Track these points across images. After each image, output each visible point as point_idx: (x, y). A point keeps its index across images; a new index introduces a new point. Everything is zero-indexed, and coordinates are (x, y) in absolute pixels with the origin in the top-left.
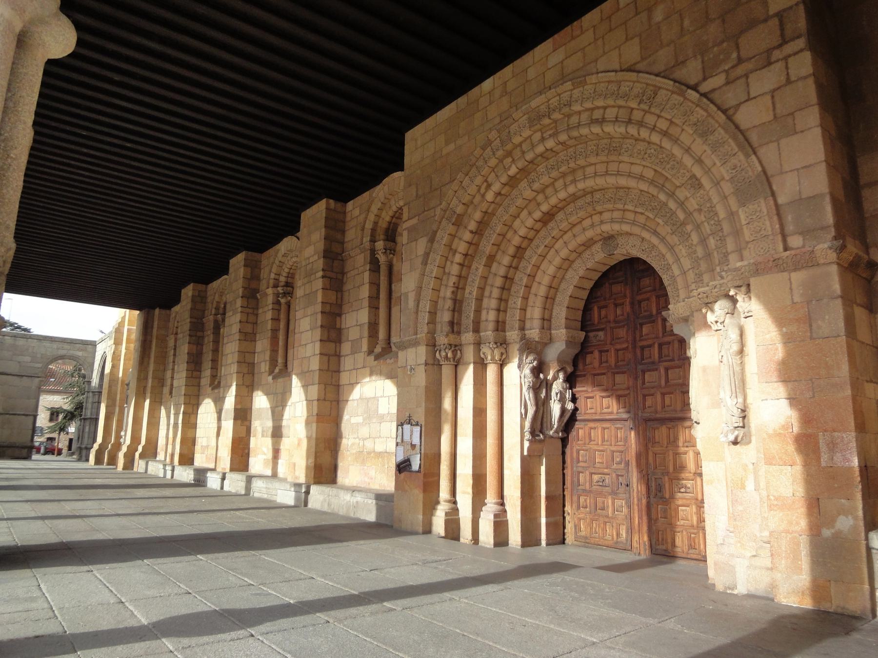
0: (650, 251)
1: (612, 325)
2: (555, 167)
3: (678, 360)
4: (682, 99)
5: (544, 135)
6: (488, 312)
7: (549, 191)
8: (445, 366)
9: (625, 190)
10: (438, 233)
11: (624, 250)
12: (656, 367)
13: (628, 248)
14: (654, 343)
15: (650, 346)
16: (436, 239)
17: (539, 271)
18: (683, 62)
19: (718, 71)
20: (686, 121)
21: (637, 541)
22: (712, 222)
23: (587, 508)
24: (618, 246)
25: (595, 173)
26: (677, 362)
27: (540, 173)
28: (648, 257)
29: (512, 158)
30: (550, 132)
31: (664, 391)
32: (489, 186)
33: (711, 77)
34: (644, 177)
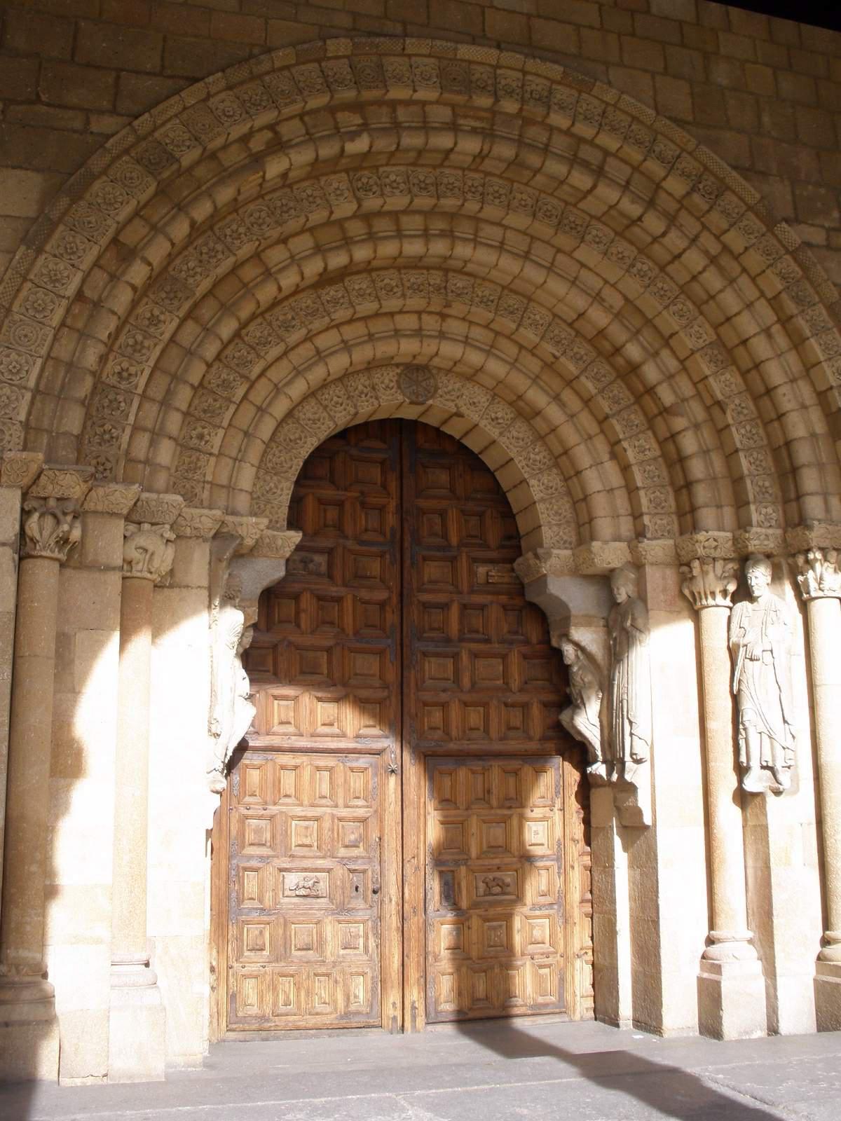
0: (509, 426)
1: (350, 544)
3: (499, 643)
4: (764, 229)
5: (461, 121)
7: (383, 225)
8: (46, 562)
9: (521, 298)
10: (97, 186)
11: (452, 404)
12: (455, 650)
13: (460, 403)
14: (452, 601)
15: (445, 607)
16: (87, 196)
17: (263, 380)
18: (764, 174)
19: (817, 222)
20: (771, 265)
21: (394, 1004)
23: (262, 950)
24: (436, 391)
25: (502, 243)
26: (497, 646)
27: (387, 181)
28: (501, 434)
29: (364, 118)
30: (477, 124)
31: (467, 698)
32: (278, 145)
33: (806, 223)
34: (603, 300)
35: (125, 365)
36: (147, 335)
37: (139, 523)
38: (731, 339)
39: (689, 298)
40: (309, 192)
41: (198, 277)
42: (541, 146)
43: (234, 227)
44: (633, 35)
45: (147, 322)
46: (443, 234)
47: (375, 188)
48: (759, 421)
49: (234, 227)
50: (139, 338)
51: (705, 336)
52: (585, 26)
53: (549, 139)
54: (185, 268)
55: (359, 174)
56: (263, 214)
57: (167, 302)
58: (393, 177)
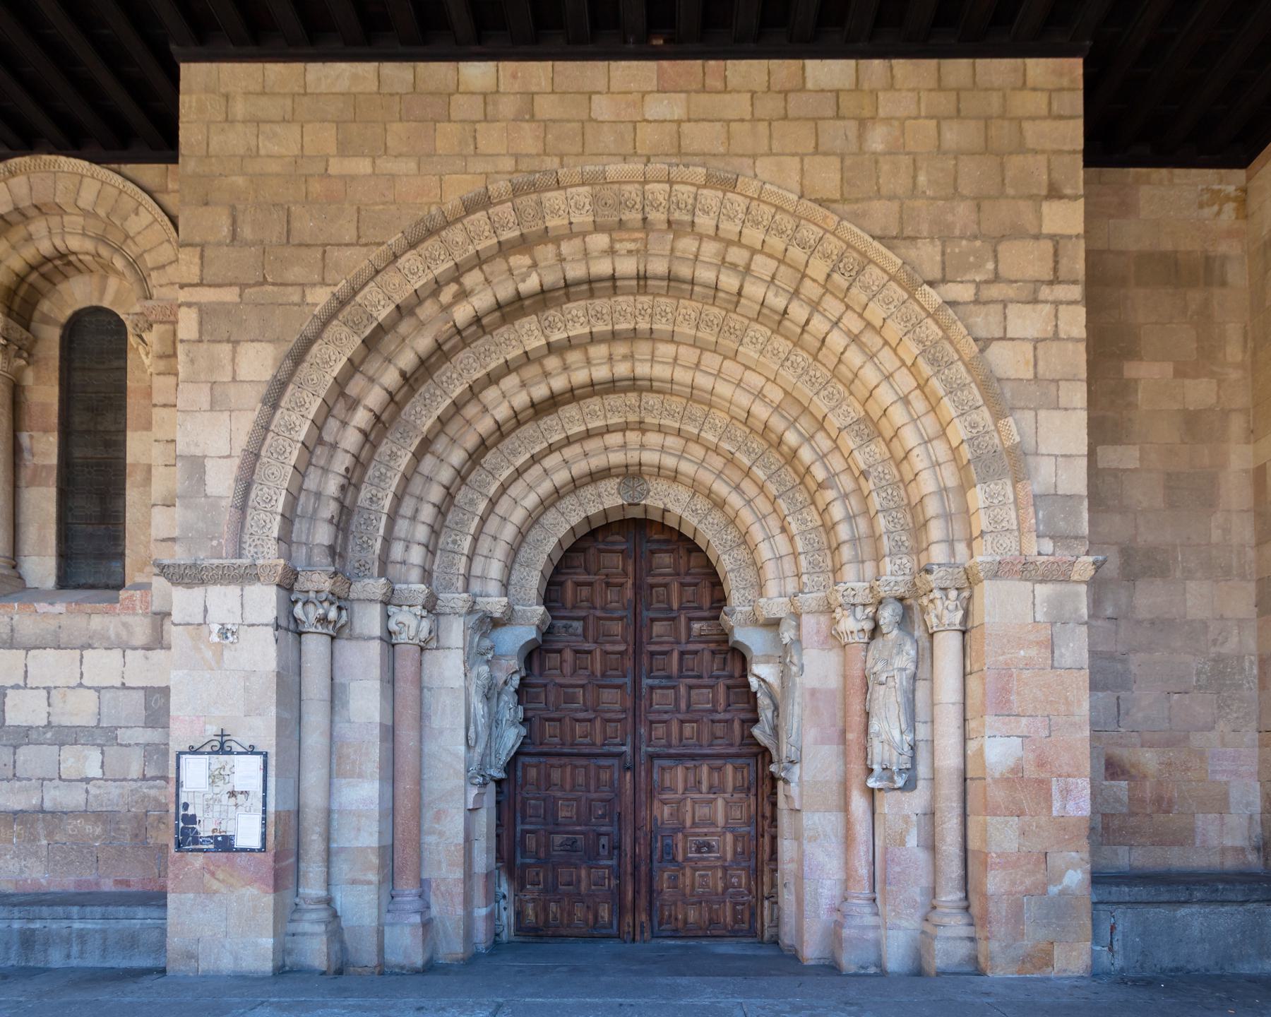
2: (606, 317)
5: (617, 246)
6: (407, 547)
22: (884, 495)
27: (569, 317)
30: (632, 246)
35: (374, 492)
36: (389, 468)
37: (400, 606)
38: (876, 413)
39: (840, 381)
40: (506, 336)
41: (424, 418)
42: (691, 257)
43: (449, 374)
44: (785, 118)
45: (388, 458)
46: (625, 358)
47: (559, 325)
48: (901, 485)
49: (449, 374)
50: (383, 470)
51: (853, 414)
52: (735, 121)
53: (699, 249)
54: (413, 412)
55: (547, 314)
56: (471, 360)
57: (402, 440)
58: (574, 312)
